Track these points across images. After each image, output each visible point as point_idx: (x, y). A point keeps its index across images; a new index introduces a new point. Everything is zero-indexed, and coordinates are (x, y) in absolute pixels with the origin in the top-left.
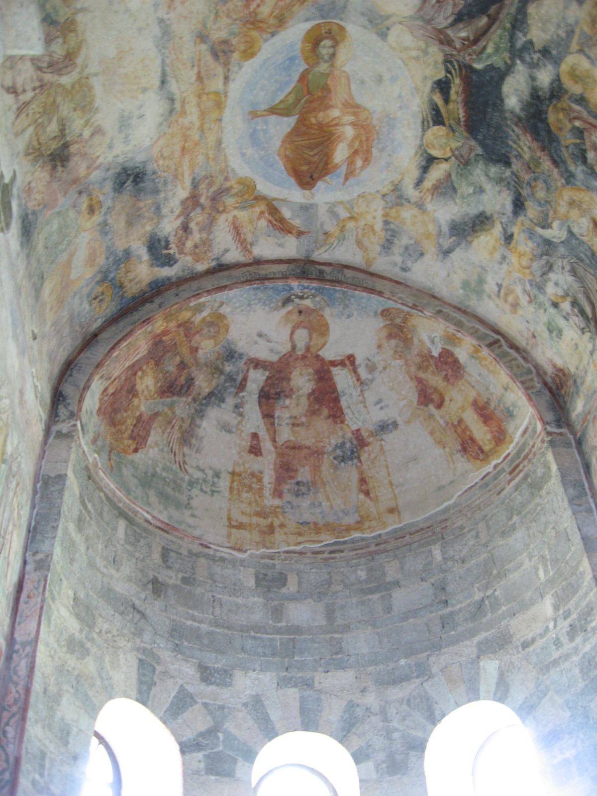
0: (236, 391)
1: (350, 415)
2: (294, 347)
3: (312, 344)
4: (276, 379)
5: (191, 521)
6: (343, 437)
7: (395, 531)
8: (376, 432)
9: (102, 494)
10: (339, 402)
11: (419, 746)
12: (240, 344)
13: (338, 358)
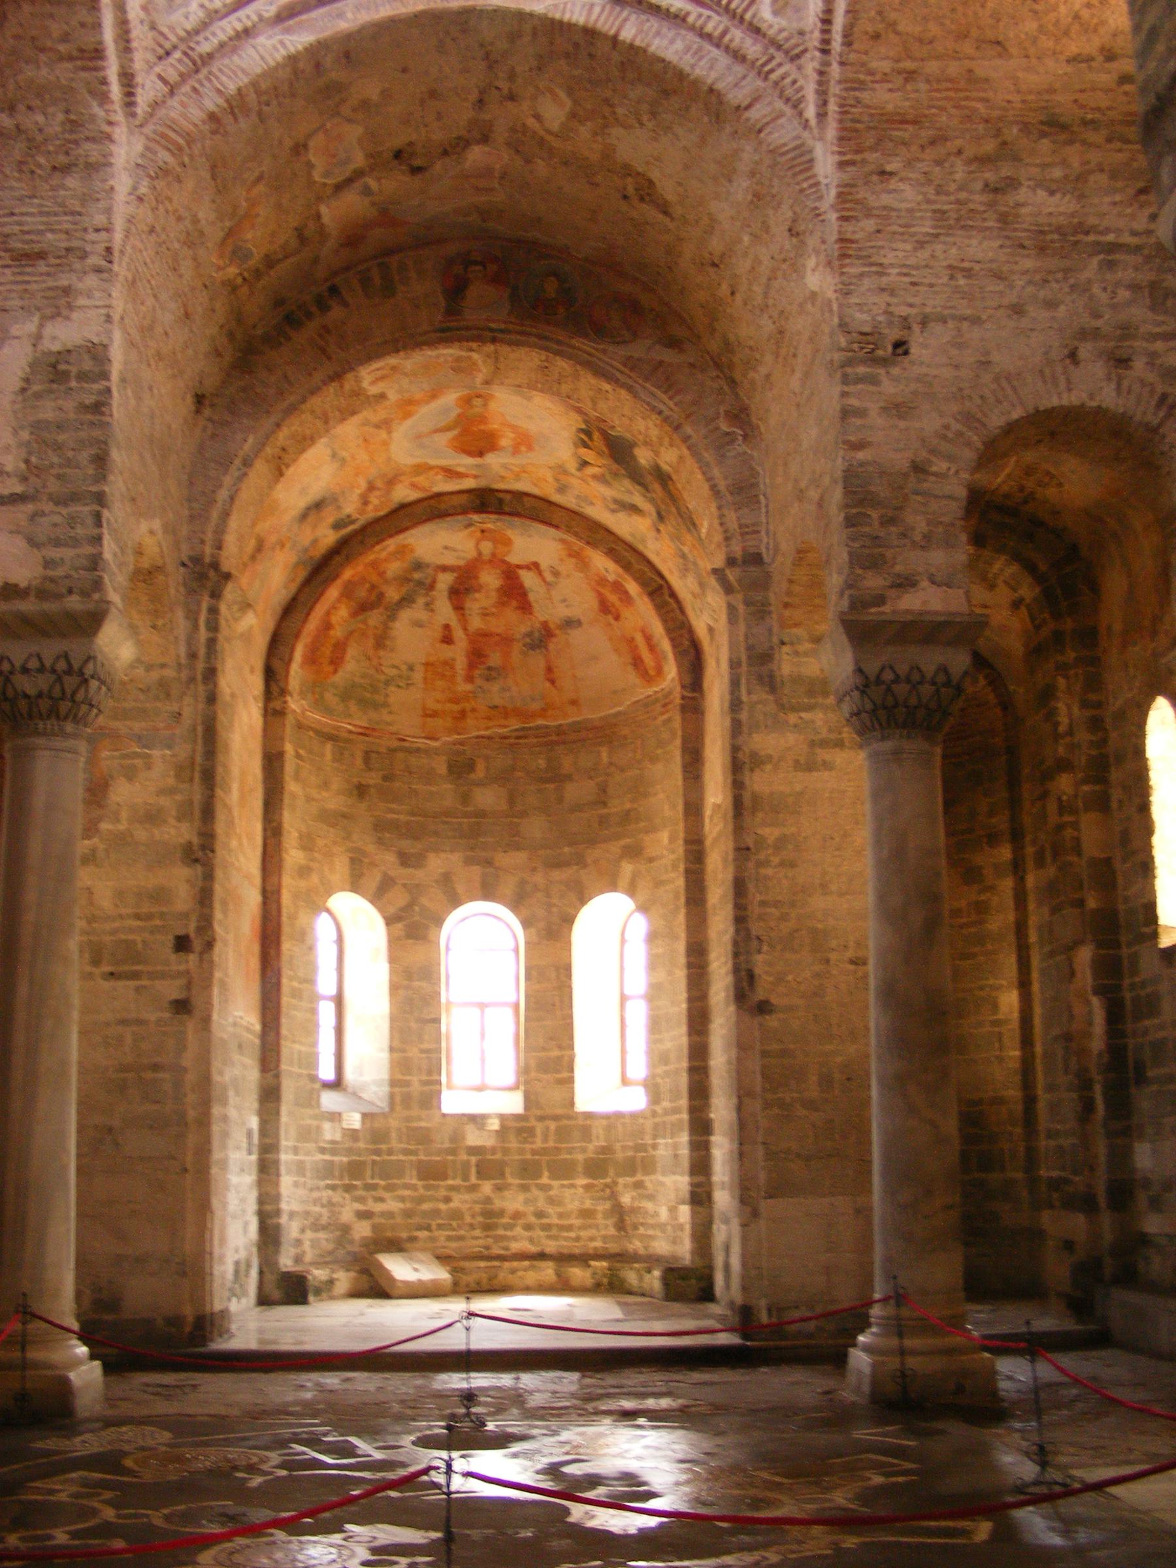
2: (480, 554)
5: (388, 718)
7: (575, 723)
9: (311, 733)
11: (569, 920)
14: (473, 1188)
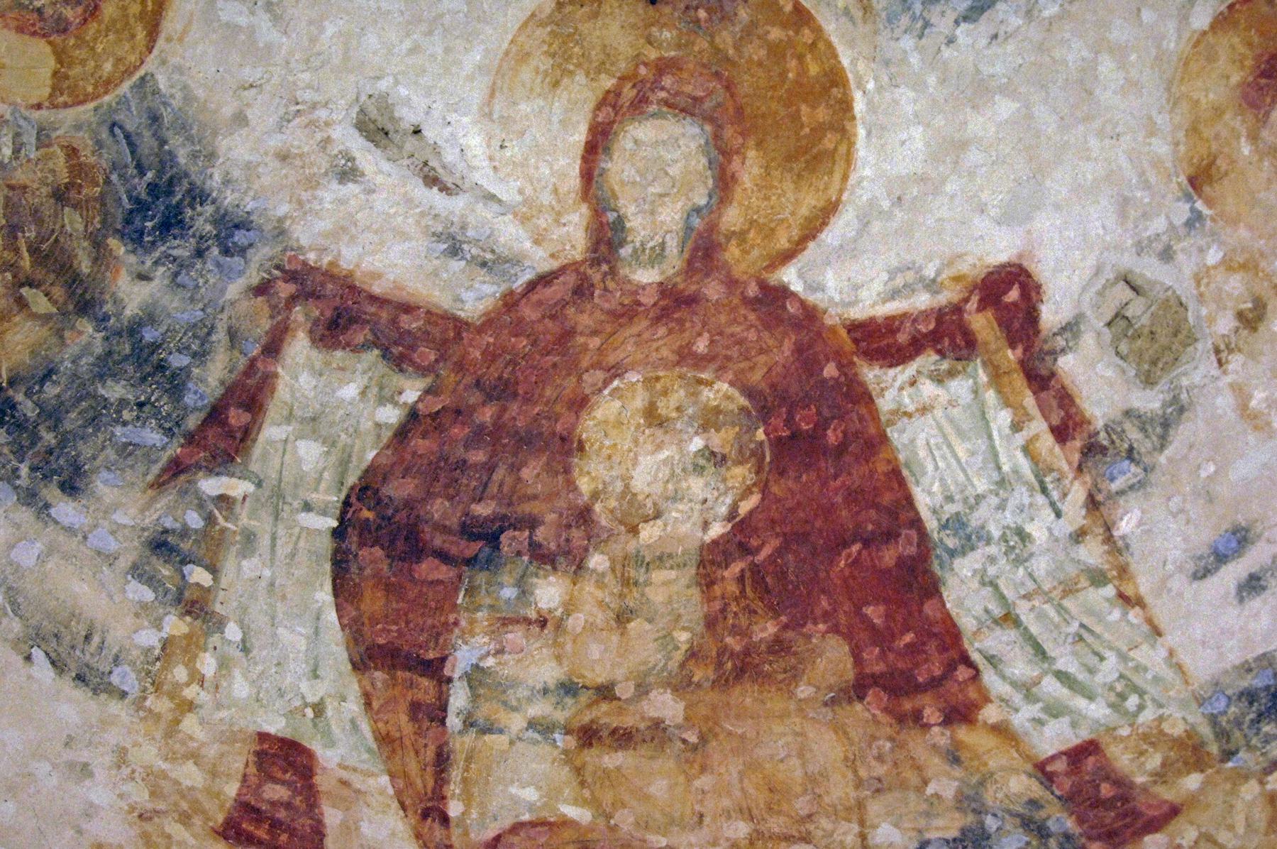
0: (176, 449)
1: (1021, 667)
2: (607, 238)
3: (732, 218)
4: (477, 435)
6: (969, 801)
8: (1222, 734)
10: (932, 589)
12: (236, 150)
13: (923, 301)
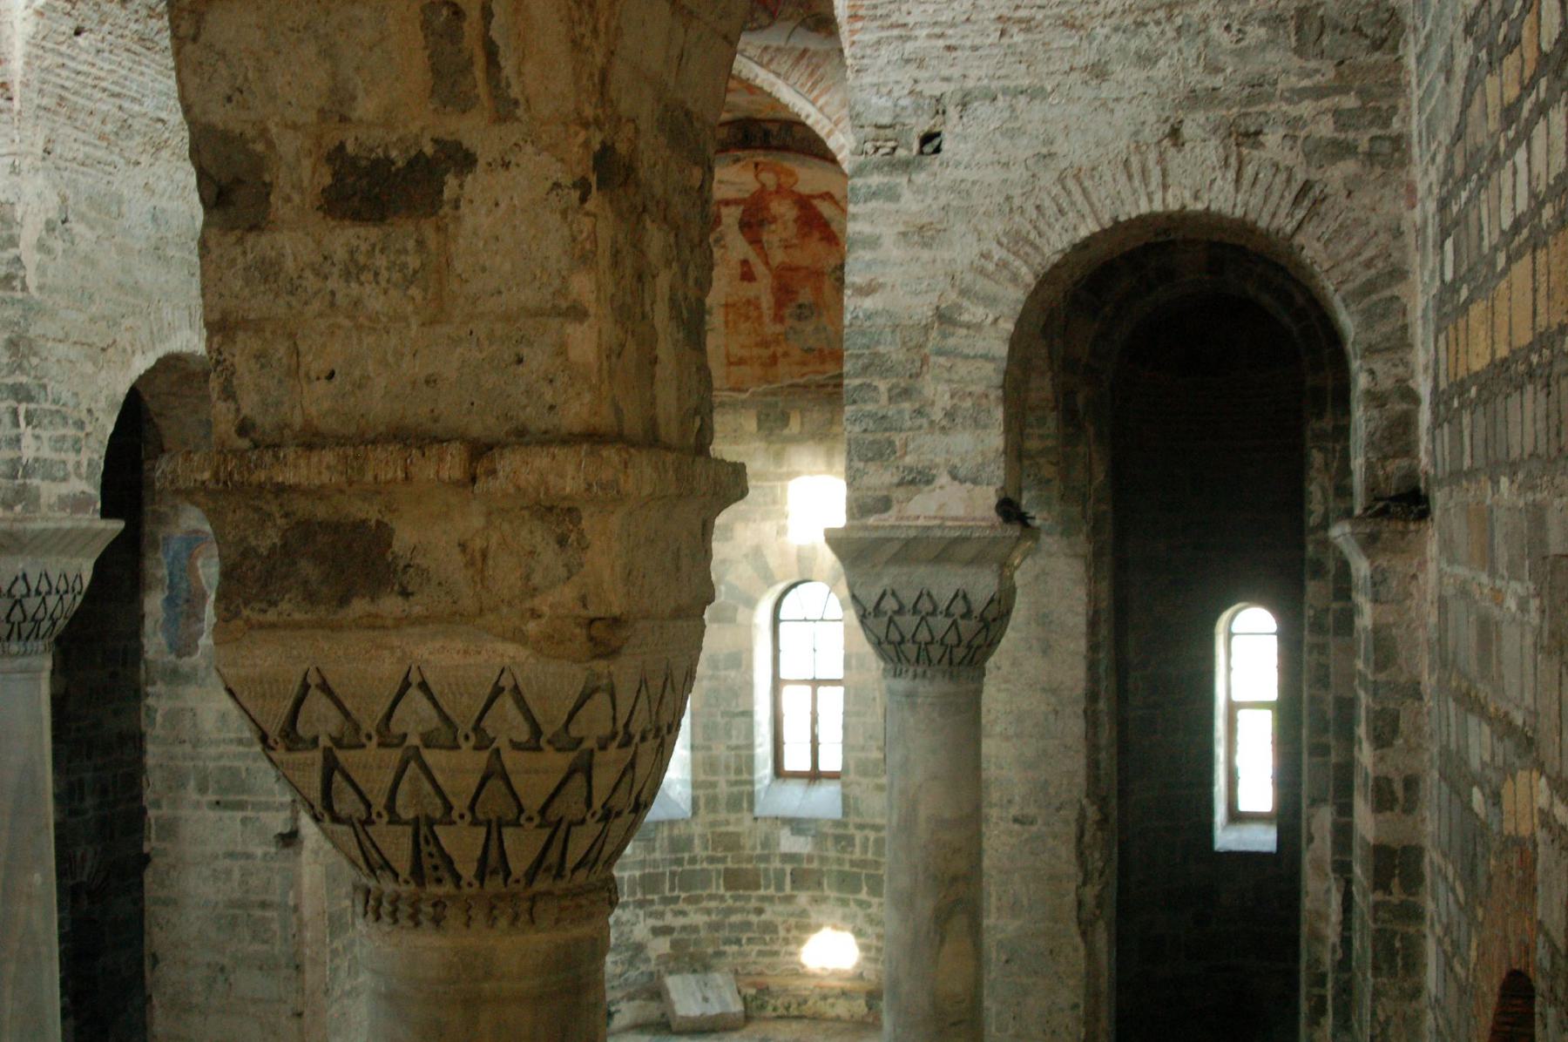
2: (763, 185)
14: (789, 899)
